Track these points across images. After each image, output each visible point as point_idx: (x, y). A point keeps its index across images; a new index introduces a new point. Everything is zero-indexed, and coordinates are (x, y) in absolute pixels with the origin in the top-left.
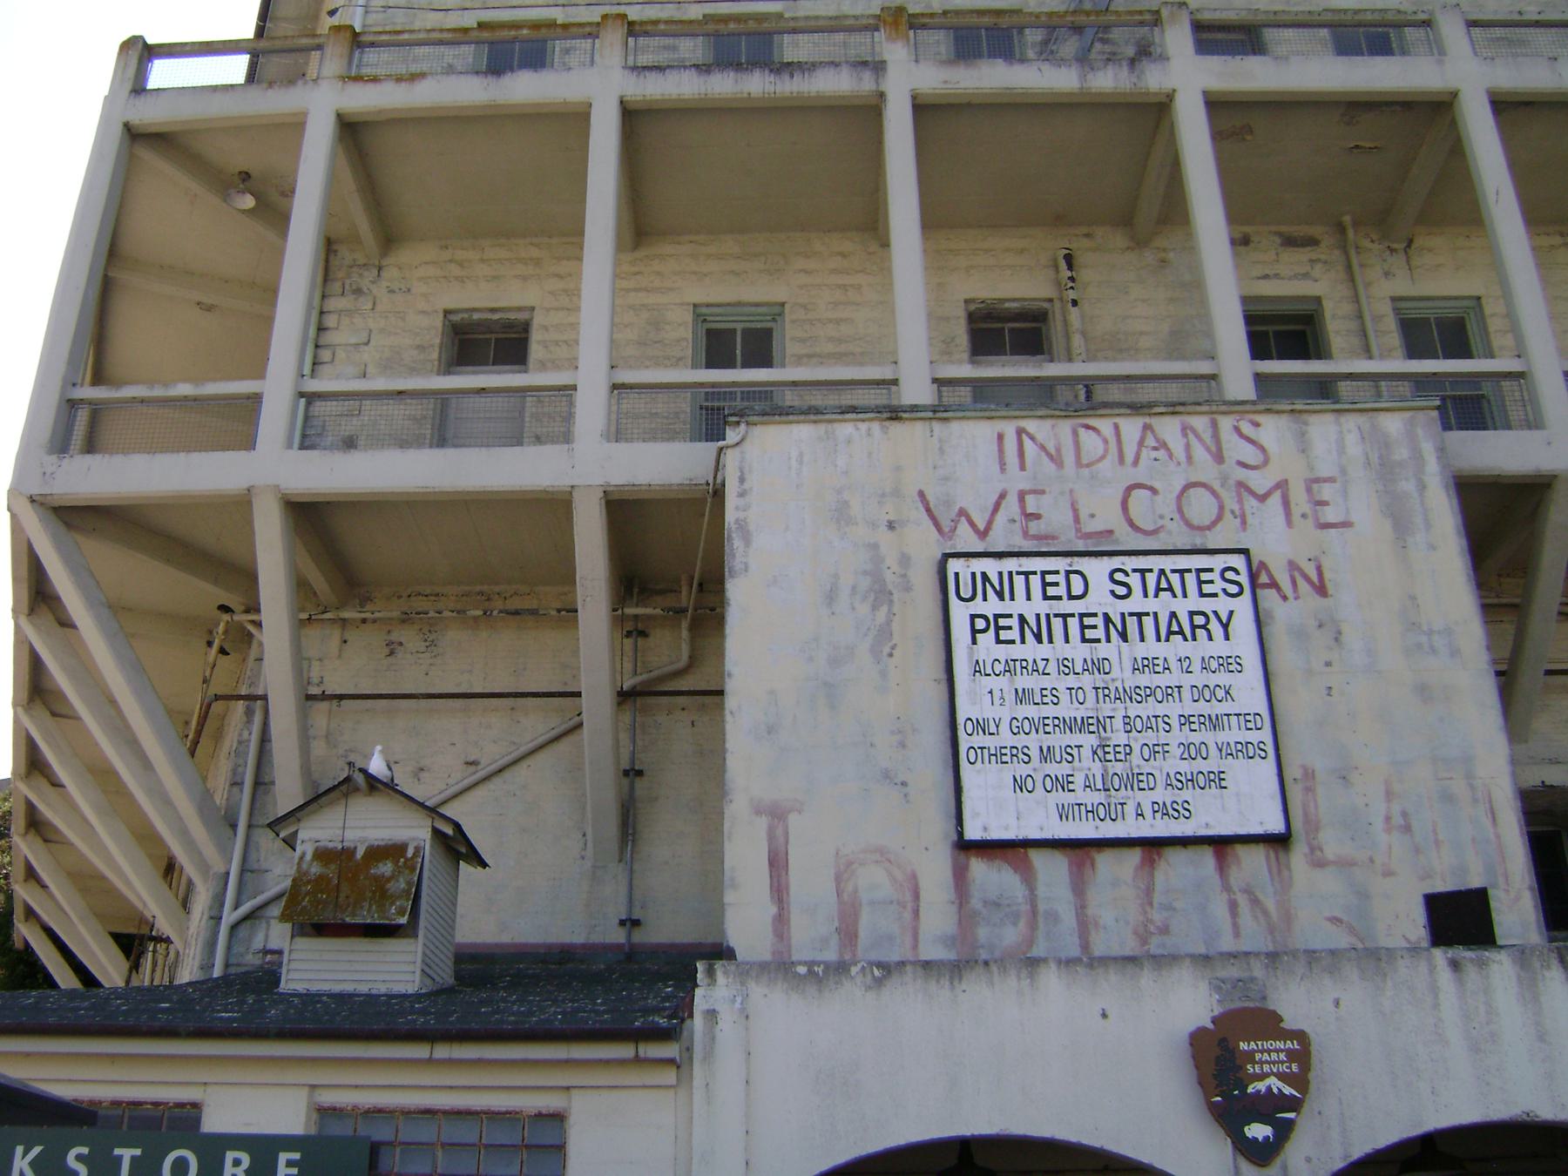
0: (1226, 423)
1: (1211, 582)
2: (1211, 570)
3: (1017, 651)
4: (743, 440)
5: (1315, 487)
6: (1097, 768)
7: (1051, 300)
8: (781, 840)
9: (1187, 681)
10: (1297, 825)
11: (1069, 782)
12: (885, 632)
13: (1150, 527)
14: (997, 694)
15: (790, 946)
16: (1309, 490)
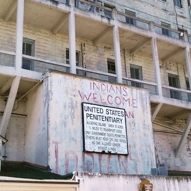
0: (122, 87)
1: (120, 114)
6: (104, 141)
7: (80, 52)
9: (116, 129)
12: (73, 114)
16: (132, 101)
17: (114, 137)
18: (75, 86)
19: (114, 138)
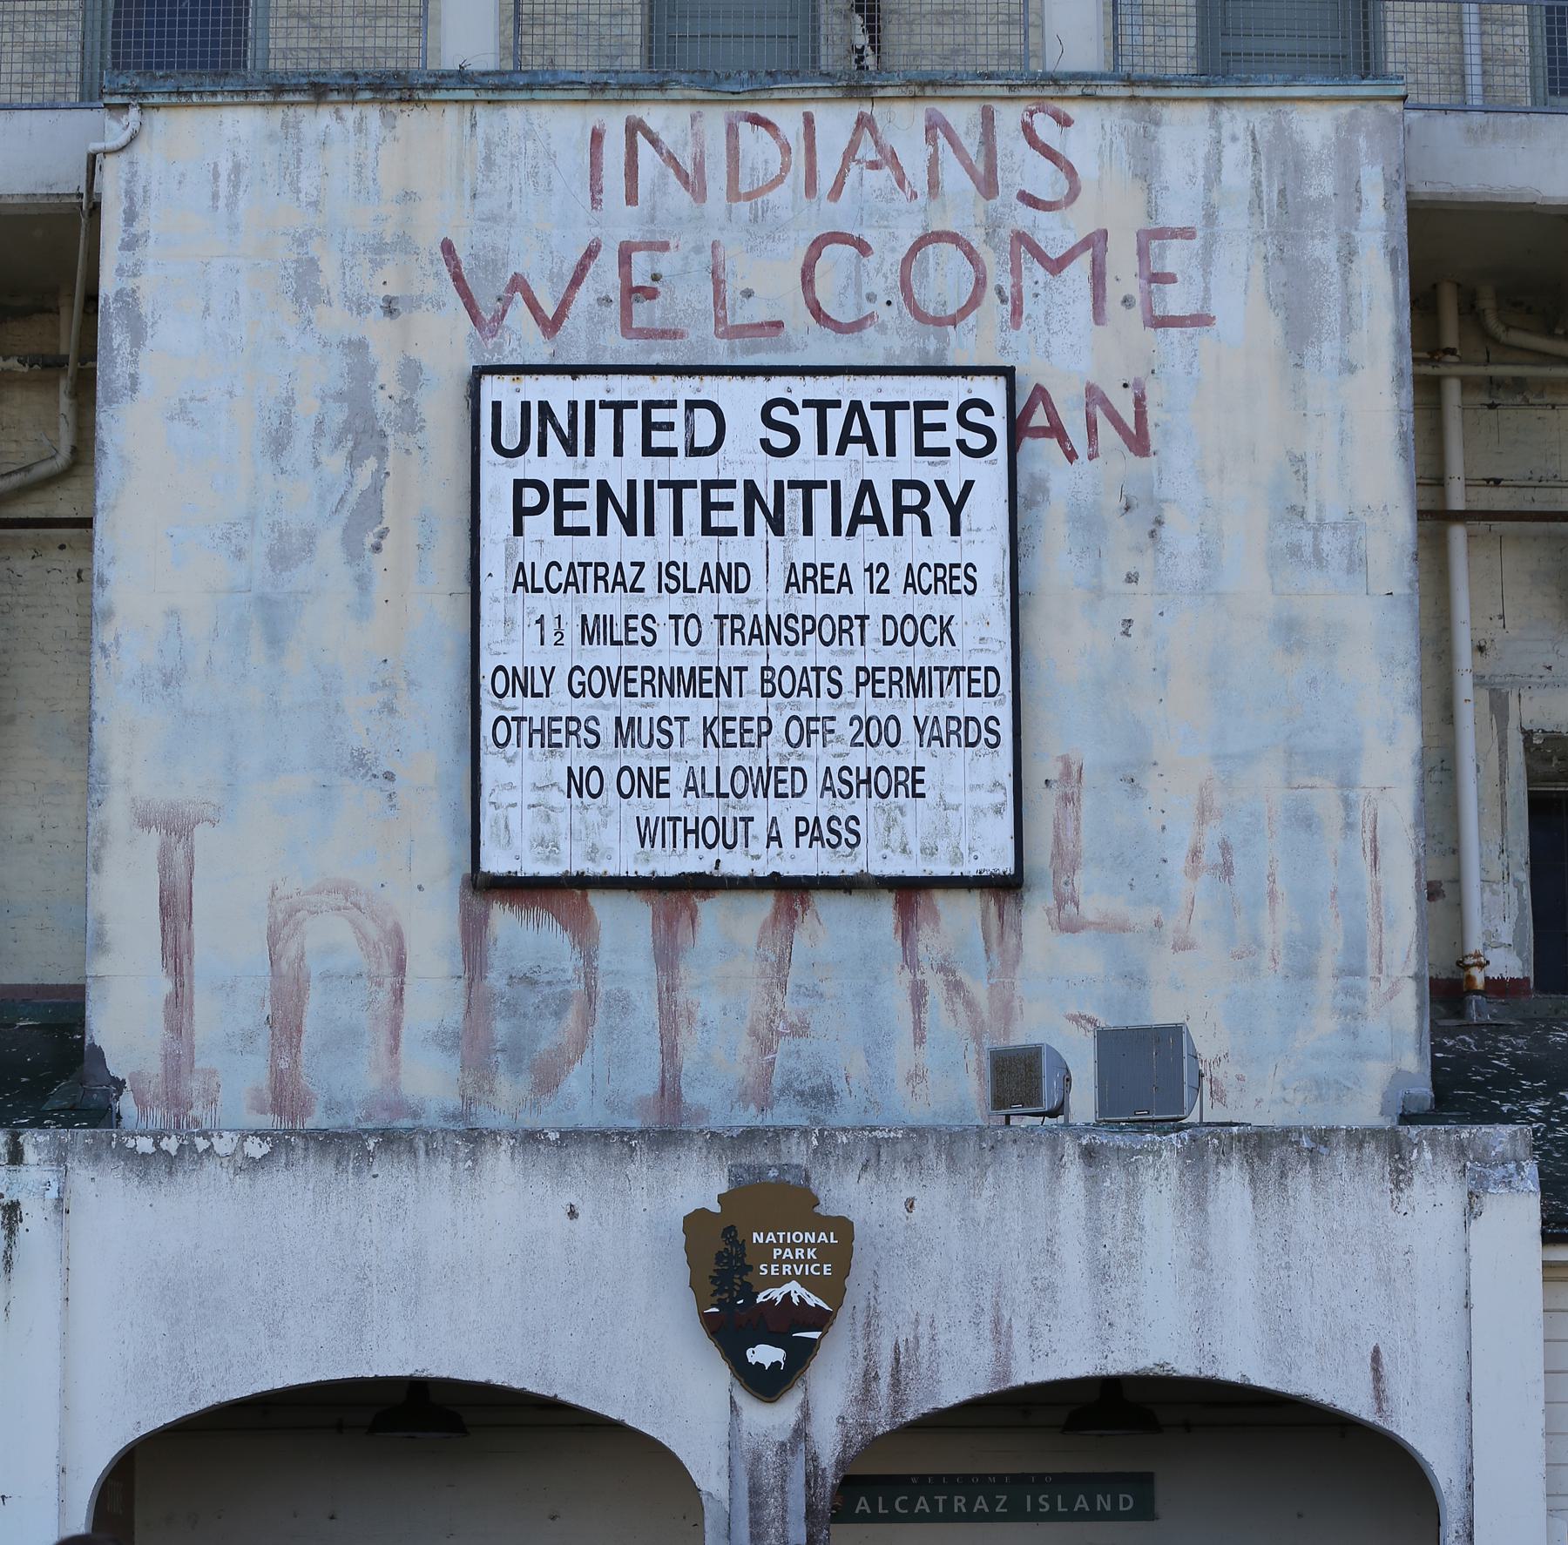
0: (1009, 117)
1: (941, 427)
2: (943, 405)
3: (588, 548)
4: (133, 139)
5: (1155, 244)
6: (710, 758)
8: (181, 870)
9: (876, 606)
10: (1040, 857)
11: (660, 781)
12: (369, 509)
13: (846, 317)
14: (550, 626)
15: (192, 1047)
16: (1143, 253)
17: (848, 695)
18: (408, 196)
19: (844, 716)
